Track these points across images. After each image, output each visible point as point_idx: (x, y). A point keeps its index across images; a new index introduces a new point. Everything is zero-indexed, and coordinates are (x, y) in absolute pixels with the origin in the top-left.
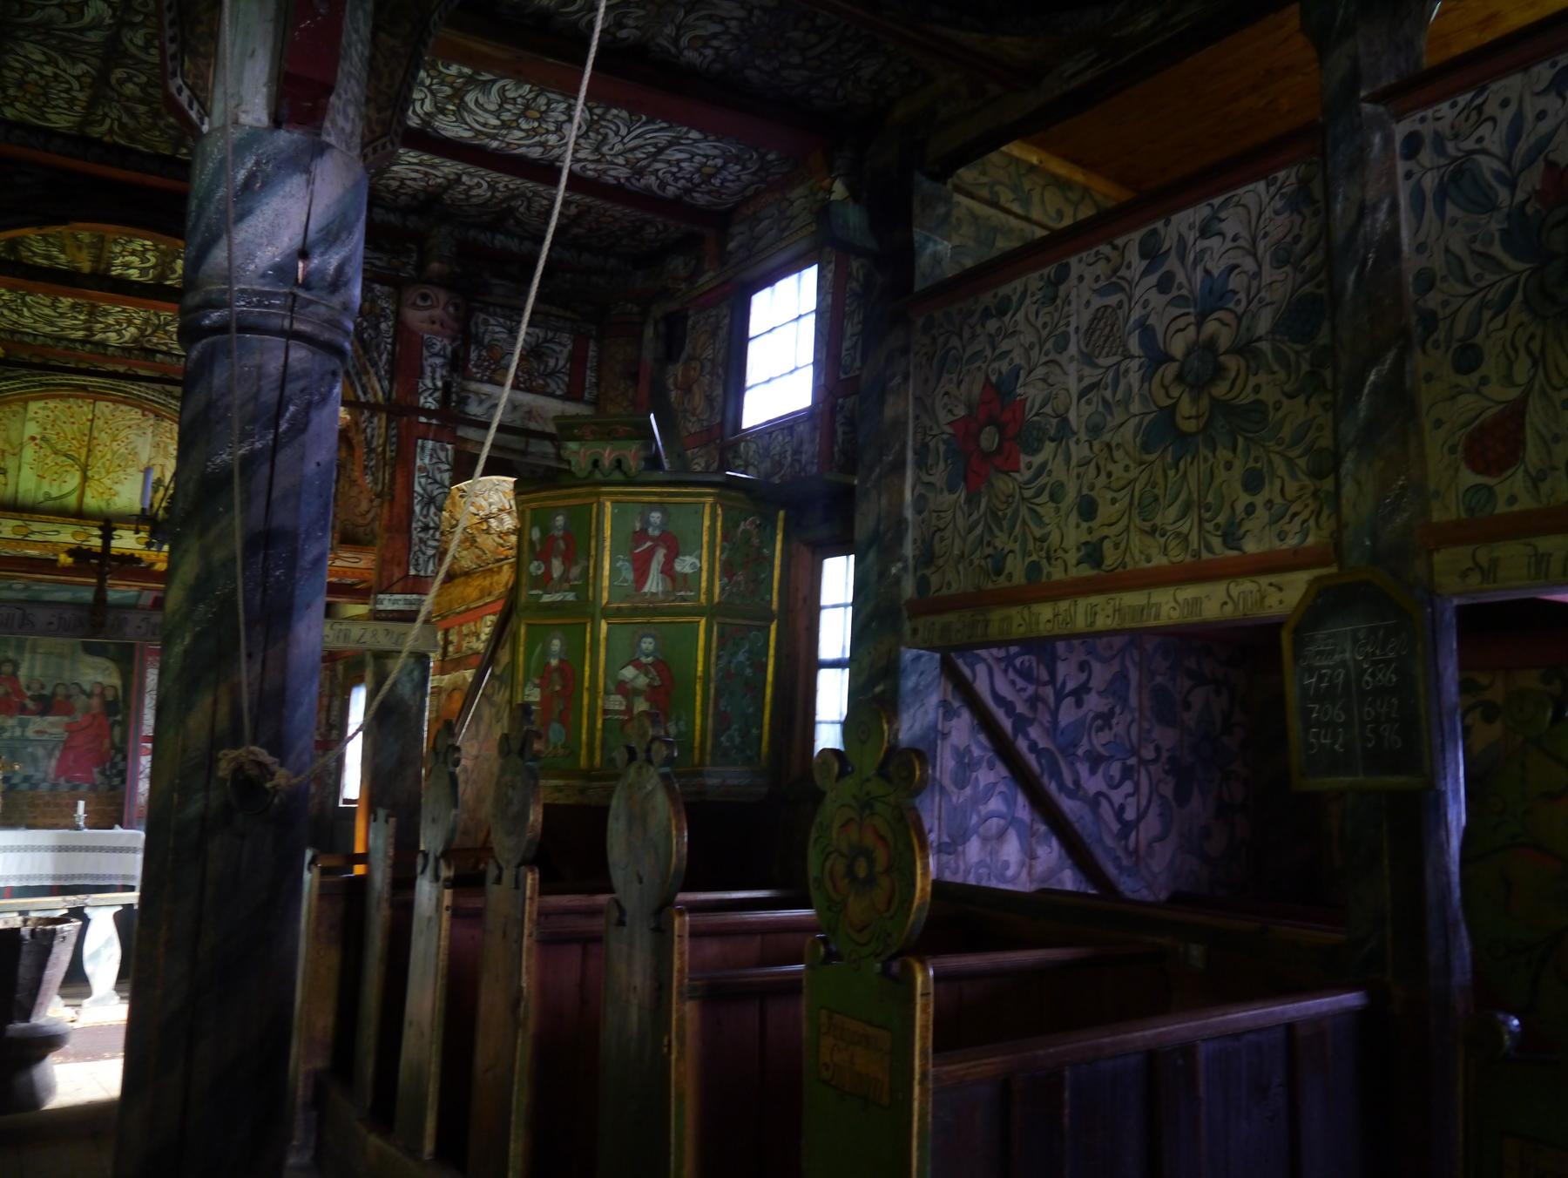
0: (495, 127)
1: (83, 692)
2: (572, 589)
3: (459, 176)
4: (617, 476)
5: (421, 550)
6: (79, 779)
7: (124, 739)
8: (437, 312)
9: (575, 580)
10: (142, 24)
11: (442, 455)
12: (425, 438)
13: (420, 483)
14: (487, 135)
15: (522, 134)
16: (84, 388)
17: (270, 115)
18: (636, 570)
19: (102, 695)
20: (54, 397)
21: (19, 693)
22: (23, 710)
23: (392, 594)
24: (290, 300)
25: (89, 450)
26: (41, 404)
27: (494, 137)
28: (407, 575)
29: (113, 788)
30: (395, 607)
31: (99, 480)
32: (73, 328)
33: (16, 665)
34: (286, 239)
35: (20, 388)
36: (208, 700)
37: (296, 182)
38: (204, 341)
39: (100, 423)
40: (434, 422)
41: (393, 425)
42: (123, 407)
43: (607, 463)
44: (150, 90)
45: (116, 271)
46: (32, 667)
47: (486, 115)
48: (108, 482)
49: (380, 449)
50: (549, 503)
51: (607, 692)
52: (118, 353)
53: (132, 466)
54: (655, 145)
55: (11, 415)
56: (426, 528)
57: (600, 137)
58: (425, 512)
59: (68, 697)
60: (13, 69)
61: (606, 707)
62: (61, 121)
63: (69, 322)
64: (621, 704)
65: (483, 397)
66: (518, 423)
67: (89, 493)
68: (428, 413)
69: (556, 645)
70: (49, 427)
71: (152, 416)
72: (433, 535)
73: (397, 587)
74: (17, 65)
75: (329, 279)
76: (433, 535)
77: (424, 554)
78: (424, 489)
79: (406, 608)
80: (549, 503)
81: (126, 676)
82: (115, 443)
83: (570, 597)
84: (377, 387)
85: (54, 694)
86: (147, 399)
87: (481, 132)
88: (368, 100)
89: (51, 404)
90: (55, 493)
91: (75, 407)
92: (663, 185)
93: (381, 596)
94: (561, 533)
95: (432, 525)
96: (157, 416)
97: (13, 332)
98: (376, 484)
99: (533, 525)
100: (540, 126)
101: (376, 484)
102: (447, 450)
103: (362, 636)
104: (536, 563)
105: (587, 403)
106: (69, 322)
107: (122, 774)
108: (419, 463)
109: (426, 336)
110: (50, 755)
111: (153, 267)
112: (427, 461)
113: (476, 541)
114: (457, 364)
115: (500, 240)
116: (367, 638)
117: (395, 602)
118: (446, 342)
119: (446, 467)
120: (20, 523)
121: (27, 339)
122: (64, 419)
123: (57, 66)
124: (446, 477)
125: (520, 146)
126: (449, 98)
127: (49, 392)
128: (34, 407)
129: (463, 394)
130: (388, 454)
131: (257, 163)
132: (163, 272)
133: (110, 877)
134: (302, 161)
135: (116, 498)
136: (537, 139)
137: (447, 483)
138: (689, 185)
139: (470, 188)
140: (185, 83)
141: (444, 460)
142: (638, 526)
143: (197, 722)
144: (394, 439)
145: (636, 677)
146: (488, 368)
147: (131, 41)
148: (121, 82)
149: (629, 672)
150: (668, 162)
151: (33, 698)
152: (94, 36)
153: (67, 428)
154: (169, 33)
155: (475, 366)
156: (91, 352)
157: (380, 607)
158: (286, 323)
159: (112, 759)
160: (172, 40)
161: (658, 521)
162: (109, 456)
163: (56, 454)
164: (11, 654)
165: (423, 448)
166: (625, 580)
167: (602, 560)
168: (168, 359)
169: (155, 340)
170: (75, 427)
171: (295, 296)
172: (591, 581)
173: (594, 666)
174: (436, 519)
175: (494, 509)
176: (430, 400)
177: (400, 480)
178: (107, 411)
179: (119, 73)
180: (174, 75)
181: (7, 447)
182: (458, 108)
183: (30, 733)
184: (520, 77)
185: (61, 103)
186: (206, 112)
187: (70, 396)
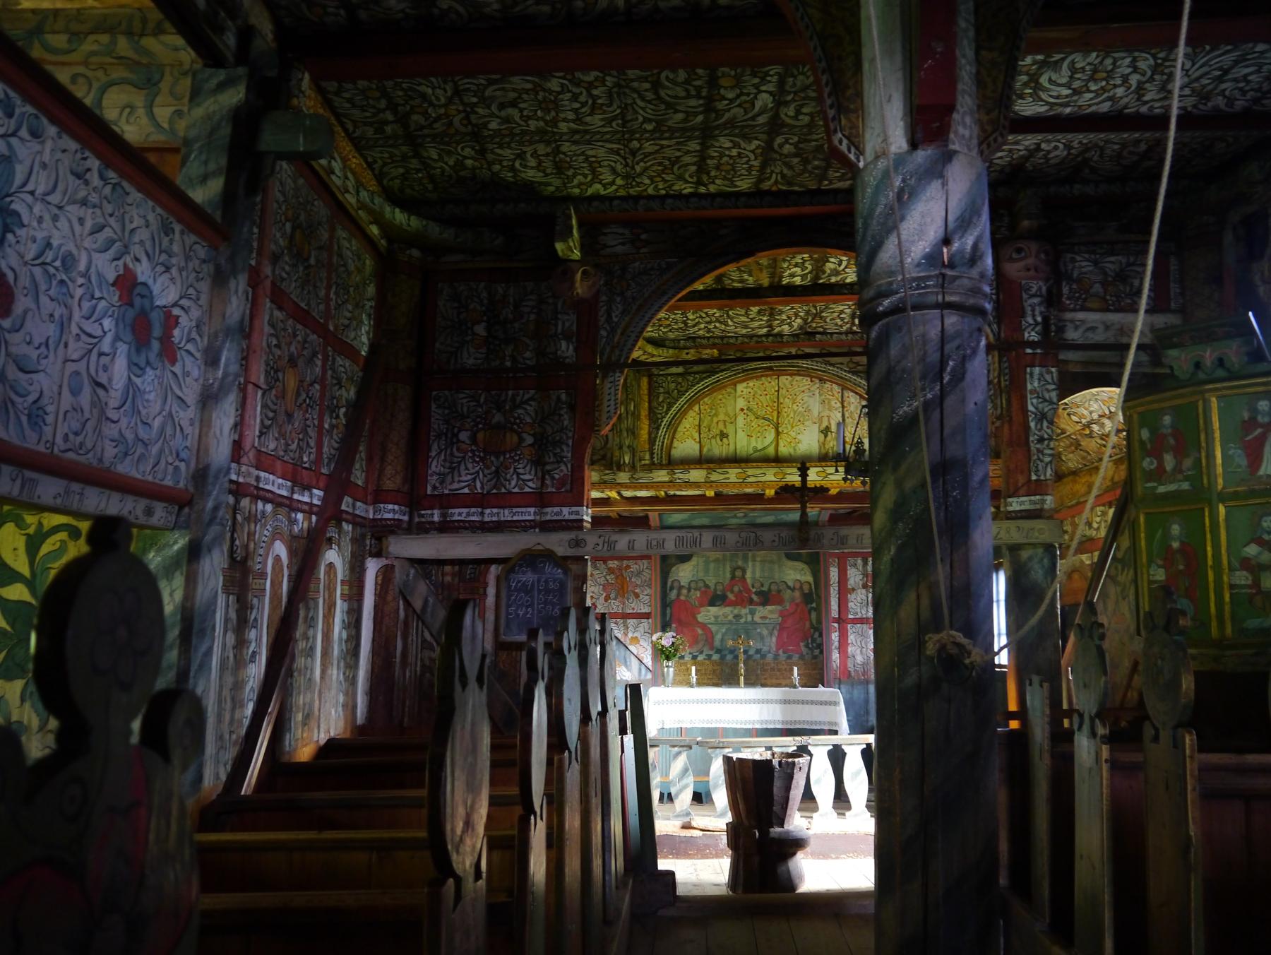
0: (1067, 96)
1: (789, 587)
2: (1186, 479)
3: (1038, 145)
4: (1221, 373)
5: (1039, 459)
7: (819, 621)
8: (1031, 261)
9: (1189, 470)
10: (793, 100)
11: (1048, 377)
12: (1033, 366)
14: (1061, 105)
15: (1091, 95)
16: (770, 369)
17: (908, 141)
18: (1248, 456)
19: (801, 588)
20: (752, 378)
21: (748, 591)
22: (751, 602)
24: (940, 280)
26: (745, 384)
27: (1066, 105)
28: (1030, 480)
29: (815, 657)
30: (1023, 507)
32: (760, 327)
33: (744, 571)
34: (932, 233)
36: (913, 596)
37: (934, 188)
38: (880, 323)
39: (783, 392)
40: (1039, 351)
41: (1005, 359)
42: (798, 378)
43: (1208, 363)
44: (801, 146)
45: (785, 281)
46: (754, 572)
47: (1059, 89)
48: (793, 434)
49: (996, 381)
50: (1155, 406)
51: (1231, 569)
52: (792, 339)
54: (1220, 69)
55: (726, 396)
56: (1041, 440)
57: (1165, 77)
58: (1039, 427)
59: (779, 591)
60: (713, 158)
61: (1233, 583)
62: (744, 185)
63: (757, 324)
64: (1247, 578)
65: (1078, 323)
66: (1112, 341)
67: (781, 443)
68: (1032, 344)
69: (1176, 529)
72: (1048, 445)
73: (1022, 491)
74: (716, 154)
75: (967, 256)
76: (1048, 445)
77: (1042, 461)
78: (1036, 408)
79: (1032, 507)
80: (1155, 406)
81: (815, 574)
83: (1185, 486)
84: (989, 331)
85: (770, 589)
87: (1056, 104)
88: (979, 107)
89: (751, 384)
90: (760, 447)
91: (767, 384)
92: (1230, 101)
93: (1010, 500)
94: (1169, 431)
95: (1046, 436)
96: (821, 380)
97: (722, 338)
98: (996, 409)
99: (1141, 427)
100: (1108, 83)
101: (996, 409)
102: (1052, 373)
103: (998, 533)
104: (1148, 459)
105: (1173, 312)
106: (757, 324)
107: (820, 646)
108: (1029, 387)
109: (1023, 282)
110: (771, 634)
111: (810, 273)
112: (1036, 384)
114: (1052, 300)
115: (1077, 189)
116: (1002, 534)
117: (1022, 503)
118: (1041, 283)
119: (1053, 387)
120: (740, 470)
121: (731, 341)
122: (759, 392)
123: (740, 148)
124: (1054, 395)
125: (1090, 106)
126: (1026, 85)
127: (748, 375)
128: (740, 387)
129: (1061, 324)
130: (1003, 384)
131: (904, 181)
132: (817, 273)
133: (820, 723)
134: (936, 171)
135: (800, 445)
136: (1106, 95)
137: (1055, 400)
138: (1259, 94)
139: (1049, 152)
140: (844, 135)
141: (1050, 381)
142: (1246, 416)
143: (907, 611)
144: (1007, 371)
145: (1260, 554)
146: (1079, 298)
147: (786, 115)
148: (781, 146)
149: (1252, 550)
150: (1236, 80)
151: (757, 593)
152: (762, 120)
154: (829, 102)
155: (1068, 299)
156: (773, 342)
157: (1010, 509)
158: (940, 298)
159: (812, 637)
160: (831, 107)
161: (1266, 409)
162: (792, 415)
164: (740, 563)
165: (1031, 374)
166: (1240, 466)
167: (1214, 451)
168: (824, 337)
169: (814, 325)
171: (944, 276)
172: (1204, 470)
173: (1216, 546)
174: (1049, 431)
175: (1095, 416)
176: (1033, 333)
177: (1015, 405)
178: (787, 383)
179: (779, 140)
180: (835, 131)
181: (727, 419)
182: (1034, 90)
184: (1086, 48)
185: (744, 172)
186: (860, 152)
187: (762, 376)
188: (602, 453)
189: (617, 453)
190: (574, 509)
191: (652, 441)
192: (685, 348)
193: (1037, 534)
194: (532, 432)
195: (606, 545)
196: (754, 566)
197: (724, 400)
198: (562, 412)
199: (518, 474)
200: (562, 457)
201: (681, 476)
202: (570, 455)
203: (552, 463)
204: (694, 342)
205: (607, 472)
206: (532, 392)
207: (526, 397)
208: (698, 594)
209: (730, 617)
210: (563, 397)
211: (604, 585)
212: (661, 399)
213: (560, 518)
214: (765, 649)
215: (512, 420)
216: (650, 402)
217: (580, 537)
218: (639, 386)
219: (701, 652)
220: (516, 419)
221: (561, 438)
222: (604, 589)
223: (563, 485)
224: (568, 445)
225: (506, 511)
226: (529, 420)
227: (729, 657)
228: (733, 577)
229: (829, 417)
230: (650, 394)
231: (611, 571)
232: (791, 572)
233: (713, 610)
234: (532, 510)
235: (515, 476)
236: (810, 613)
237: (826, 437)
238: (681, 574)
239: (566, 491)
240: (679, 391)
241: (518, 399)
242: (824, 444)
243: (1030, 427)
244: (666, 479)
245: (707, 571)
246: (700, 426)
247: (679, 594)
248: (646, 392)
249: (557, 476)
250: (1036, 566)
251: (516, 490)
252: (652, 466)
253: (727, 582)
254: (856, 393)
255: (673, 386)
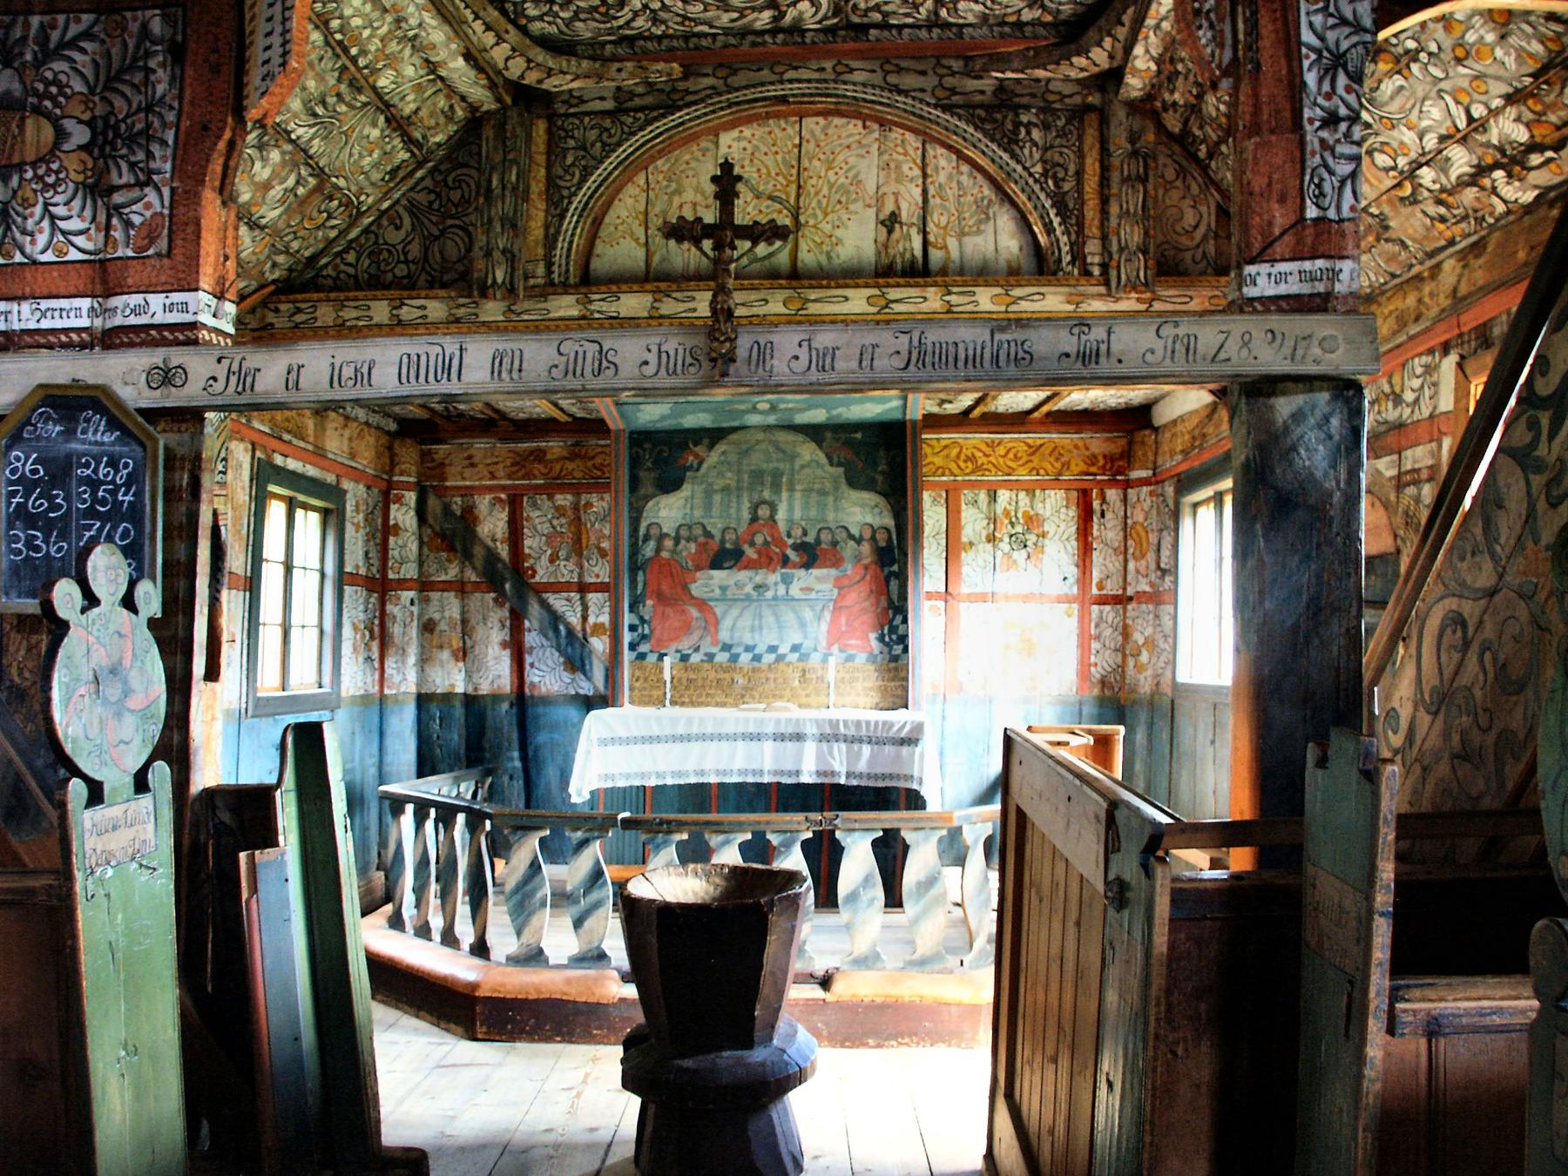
1: (852, 537)
5: (1326, 166)
6: (856, 646)
7: (903, 596)
13: (1311, 24)
16: (783, 100)
20: (749, 120)
21: (779, 542)
22: (785, 562)
23: (1273, 261)
25: (799, 187)
26: (735, 133)
28: (1302, 219)
30: (1282, 289)
31: (815, 227)
33: (773, 508)
35: (706, 114)
39: (809, 147)
42: (837, 121)
46: (791, 509)
48: (827, 228)
52: (821, 37)
53: (855, 201)
56: (1331, 120)
58: (1326, 87)
59: (835, 544)
70: (747, 162)
71: (876, 126)
72: (1347, 135)
73: (1278, 249)
76: (1347, 135)
78: (1322, 39)
79: (1305, 289)
82: (831, 173)
85: (818, 541)
86: (865, 100)
89: (747, 132)
91: (777, 131)
93: (1250, 269)
95: (1343, 111)
96: (882, 123)
97: (687, 37)
98: (1221, 46)
101: (1221, 46)
113: (1387, 228)
116: (1232, 349)
117: (1282, 278)
121: (704, 43)
122: (764, 149)
135: (839, 249)
151: (796, 547)
153: (769, 161)
156: (785, 43)
157: (1250, 292)
162: (825, 191)
163: (758, 197)
164: (767, 494)
168: (886, 33)
170: (779, 157)
174: (1351, 99)
175: (1431, 142)
177: (1267, 27)
181: (699, 198)
183: (795, 591)
187: (768, 116)
188: (460, 267)
189: (480, 264)
190: (177, 297)
191: (550, 242)
192: (615, 58)
193: (1316, 351)
194: (86, 116)
195: (233, 379)
196: (790, 498)
197: (693, 164)
198: (152, 64)
199: (53, 218)
200: (150, 172)
201: (604, 306)
202: (168, 166)
203: (128, 186)
204: (632, 48)
205: (462, 301)
206: (87, 18)
207: (74, 30)
208: (693, 547)
209: (749, 589)
210: (156, 26)
211: (548, 536)
212: (569, 160)
213: (143, 320)
214: (808, 645)
215: (41, 87)
216: (548, 168)
217: (174, 362)
218: (529, 139)
219: (697, 649)
220: (47, 83)
221: (149, 126)
222: (548, 544)
223: (152, 239)
224: (164, 143)
225: (26, 307)
226: (78, 86)
227: (745, 658)
228: (755, 519)
229: (896, 195)
230: (549, 153)
231: (561, 512)
232: (857, 509)
233: (718, 576)
234: (85, 303)
235: (46, 224)
236: (887, 581)
237: (890, 232)
238: (663, 513)
239: (159, 255)
240: (604, 145)
241: (55, 36)
242: (886, 247)
243: (1304, 84)
244: (575, 312)
245: (708, 506)
246: (646, 213)
247: (658, 550)
248: (542, 148)
249: (137, 220)
250: (1312, 436)
251: (49, 257)
252: (552, 288)
253: (743, 528)
254: (950, 148)
255: (593, 135)
